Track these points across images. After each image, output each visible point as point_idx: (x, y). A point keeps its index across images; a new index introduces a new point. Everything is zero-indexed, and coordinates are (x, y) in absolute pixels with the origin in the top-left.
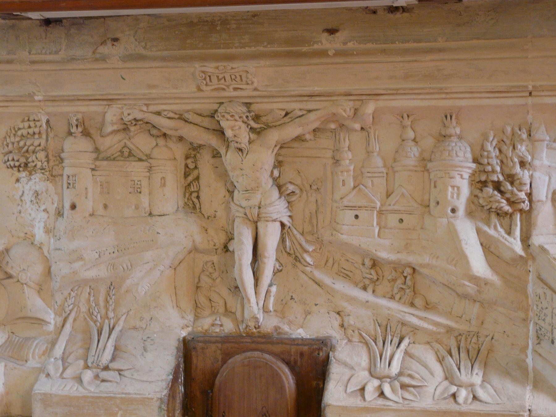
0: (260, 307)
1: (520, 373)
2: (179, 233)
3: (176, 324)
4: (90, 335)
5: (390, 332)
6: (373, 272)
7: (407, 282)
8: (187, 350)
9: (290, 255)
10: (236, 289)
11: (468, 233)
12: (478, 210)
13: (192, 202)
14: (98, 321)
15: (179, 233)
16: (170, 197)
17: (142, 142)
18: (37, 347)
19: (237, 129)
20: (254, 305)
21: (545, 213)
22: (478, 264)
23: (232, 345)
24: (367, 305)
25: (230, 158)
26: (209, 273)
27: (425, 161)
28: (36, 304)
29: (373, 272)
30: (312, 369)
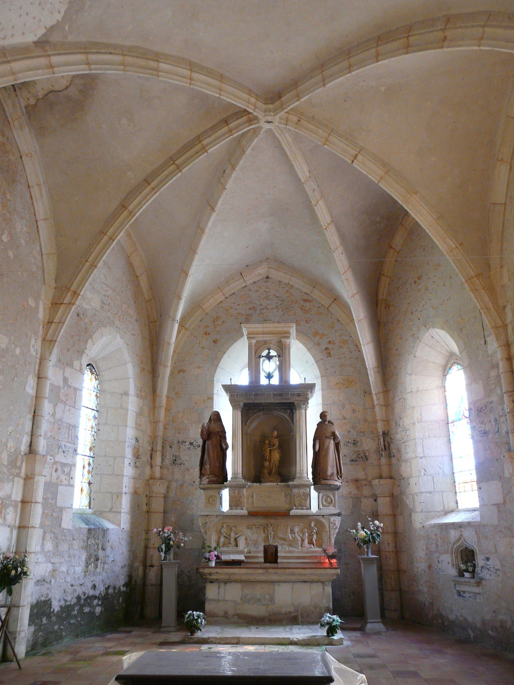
0: (271, 542)
1: (294, 547)
2: (263, 535)
3: (263, 544)
4: (255, 545)
5: (283, 544)
6: (281, 539)
7: (284, 539)
8: (264, 546)
9: (274, 537)
10: (269, 540)
11: (290, 535)
12: (291, 533)
13: (264, 532)
14: (255, 543)
15: (263, 535)
16: (262, 532)
17: (260, 526)
18: (250, 547)
19: (269, 525)
20: (270, 542)
21: (296, 533)
22: (291, 538)
23: (269, 546)
24: (281, 542)
25: (268, 528)
26: (267, 539)
27: (286, 529)
28: (249, 542)
29: (281, 539)
30: (276, 548)
